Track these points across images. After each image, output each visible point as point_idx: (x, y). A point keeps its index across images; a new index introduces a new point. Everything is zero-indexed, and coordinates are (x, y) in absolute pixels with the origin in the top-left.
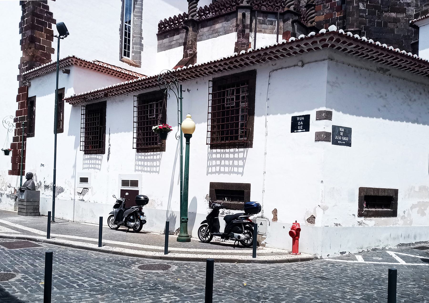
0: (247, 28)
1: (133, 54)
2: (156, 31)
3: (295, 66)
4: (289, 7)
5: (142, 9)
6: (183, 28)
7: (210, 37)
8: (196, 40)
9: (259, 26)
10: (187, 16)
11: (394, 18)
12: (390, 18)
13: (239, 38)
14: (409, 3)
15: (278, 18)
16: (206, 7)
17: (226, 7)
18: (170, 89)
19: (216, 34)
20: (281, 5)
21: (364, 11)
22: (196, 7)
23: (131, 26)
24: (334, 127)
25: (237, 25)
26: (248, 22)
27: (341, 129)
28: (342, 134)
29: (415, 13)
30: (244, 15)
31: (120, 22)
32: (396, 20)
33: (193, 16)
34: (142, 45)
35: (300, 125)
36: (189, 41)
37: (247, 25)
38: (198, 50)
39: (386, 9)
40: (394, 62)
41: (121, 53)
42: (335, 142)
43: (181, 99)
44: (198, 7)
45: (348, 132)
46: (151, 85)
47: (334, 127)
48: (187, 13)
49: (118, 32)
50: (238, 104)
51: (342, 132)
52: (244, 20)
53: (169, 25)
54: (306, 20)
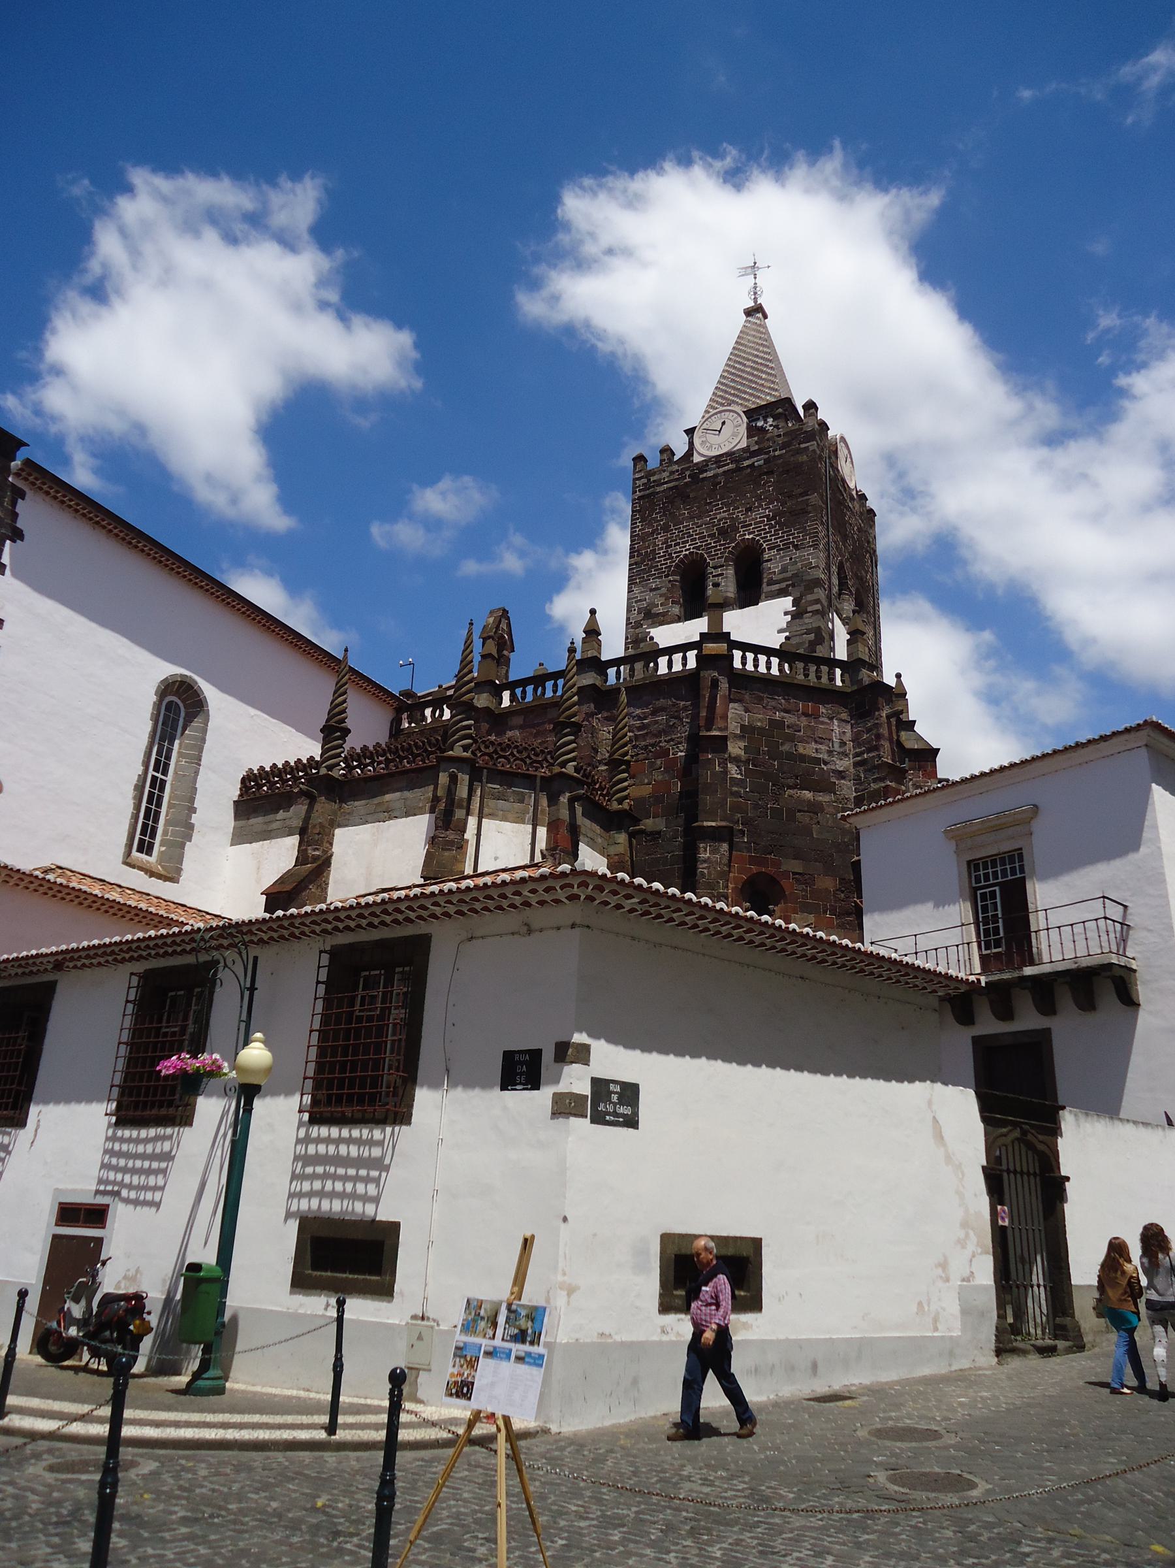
0: (461, 807)
1: (163, 849)
2: (235, 793)
3: (513, 934)
4: (563, 764)
5: (204, 740)
6: (302, 793)
7: (369, 818)
8: (334, 824)
9: (491, 803)
10: (317, 765)
12: (800, 800)
14: (841, 772)
15: (538, 788)
16: (365, 748)
17: (412, 753)
18: (226, 966)
20: (546, 759)
21: (740, 783)
22: (341, 746)
23: (169, 779)
24: (596, 1082)
25: (436, 799)
26: (462, 792)
27: (612, 1087)
28: (615, 1098)
30: (453, 779)
31: (140, 770)
32: (815, 808)
33: (330, 768)
34: (191, 827)
35: (521, 1074)
36: (314, 826)
37: (461, 799)
38: (335, 849)
39: (791, 782)
42: (598, 1119)
43: (252, 989)
44: (347, 746)
45: (630, 1093)
47: (596, 1082)
48: (318, 758)
49: (130, 792)
50: (386, 1011)
52: (453, 787)
53: (269, 781)
54: (608, 794)
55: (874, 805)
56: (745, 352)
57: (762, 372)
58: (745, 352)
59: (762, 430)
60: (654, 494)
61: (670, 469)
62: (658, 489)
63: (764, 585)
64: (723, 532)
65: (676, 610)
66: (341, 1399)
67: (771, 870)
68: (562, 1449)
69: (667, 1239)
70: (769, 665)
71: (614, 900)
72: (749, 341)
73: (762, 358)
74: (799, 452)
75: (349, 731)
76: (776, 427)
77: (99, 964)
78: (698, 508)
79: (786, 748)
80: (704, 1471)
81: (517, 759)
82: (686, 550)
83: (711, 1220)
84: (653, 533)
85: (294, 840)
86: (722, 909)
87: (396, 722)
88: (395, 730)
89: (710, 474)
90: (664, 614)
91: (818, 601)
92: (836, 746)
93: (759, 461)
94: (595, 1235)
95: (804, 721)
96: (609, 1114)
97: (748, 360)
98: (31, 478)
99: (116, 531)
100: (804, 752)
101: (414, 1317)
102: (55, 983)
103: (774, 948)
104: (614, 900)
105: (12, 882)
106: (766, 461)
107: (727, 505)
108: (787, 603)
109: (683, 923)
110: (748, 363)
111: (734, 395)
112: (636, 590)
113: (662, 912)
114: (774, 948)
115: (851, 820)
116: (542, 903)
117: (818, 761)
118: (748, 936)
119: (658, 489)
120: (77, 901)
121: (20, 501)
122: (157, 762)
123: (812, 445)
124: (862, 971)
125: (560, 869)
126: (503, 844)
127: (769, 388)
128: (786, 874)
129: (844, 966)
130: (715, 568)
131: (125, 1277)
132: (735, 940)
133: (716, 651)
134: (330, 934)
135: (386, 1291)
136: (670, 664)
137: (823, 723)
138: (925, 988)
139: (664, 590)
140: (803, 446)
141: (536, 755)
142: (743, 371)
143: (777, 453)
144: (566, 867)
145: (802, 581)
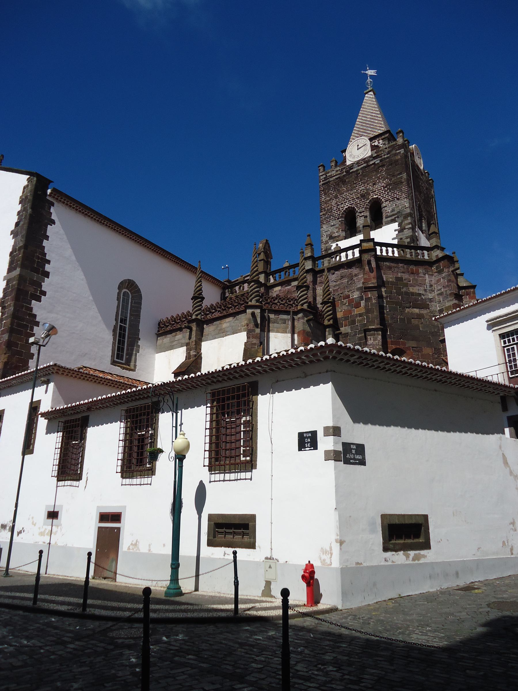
4: (302, 305)
7: (217, 336)
11: (417, 314)
13: (248, 337)
19: (223, 333)
20: (294, 303)
22: (201, 305)
24: (344, 444)
27: (352, 446)
29: (438, 309)
31: (114, 323)
32: (420, 317)
33: (197, 315)
35: (308, 443)
39: (408, 305)
40: (404, 370)
41: (113, 356)
42: (347, 462)
45: (361, 449)
46: (142, 397)
47: (344, 444)
48: (191, 312)
51: (354, 449)
55: (459, 309)
56: (366, 111)
57: (375, 120)
58: (366, 111)
59: (377, 146)
60: (329, 182)
61: (336, 169)
62: (331, 179)
63: (384, 218)
64: (363, 196)
65: (344, 234)
66: (239, 597)
67: (401, 347)
68: (346, 618)
69: (383, 516)
70: (393, 252)
71: (346, 358)
72: (368, 106)
73: (375, 113)
74: (396, 154)
75: (204, 298)
76: (384, 144)
77: (107, 407)
78: (350, 186)
79: (404, 290)
80: (420, 628)
81: (281, 304)
82: (346, 205)
83: (406, 507)
84: (330, 200)
85: (184, 349)
86: (397, 359)
87: (223, 294)
88: (223, 297)
89: (355, 170)
91: (409, 224)
92: (428, 287)
93: (377, 161)
94: (350, 517)
96: (352, 459)
97: (368, 115)
98: (56, 197)
99: (94, 217)
100: (413, 291)
101: (267, 558)
102: (88, 416)
103: (422, 376)
104: (346, 358)
105: (65, 374)
106: (381, 161)
107: (364, 183)
108: (395, 226)
109: (379, 367)
110: (368, 117)
111: (363, 132)
113: (369, 362)
114: (422, 376)
115: (439, 320)
116: (311, 362)
117: (420, 295)
118: (409, 372)
119: (331, 179)
120: (94, 380)
121: (52, 207)
123: (402, 151)
124: (464, 385)
125: (319, 344)
126: (280, 343)
127: (379, 127)
128: (408, 348)
129: (455, 383)
130: (360, 213)
131: (132, 544)
132: (403, 374)
133: (368, 247)
134: (210, 384)
135: (252, 546)
136: (347, 256)
137: (421, 277)
138: (494, 392)
139: (337, 225)
140: (397, 152)
141: (290, 302)
142: (366, 120)
143: (385, 157)
144: (322, 343)
145: (402, 215)
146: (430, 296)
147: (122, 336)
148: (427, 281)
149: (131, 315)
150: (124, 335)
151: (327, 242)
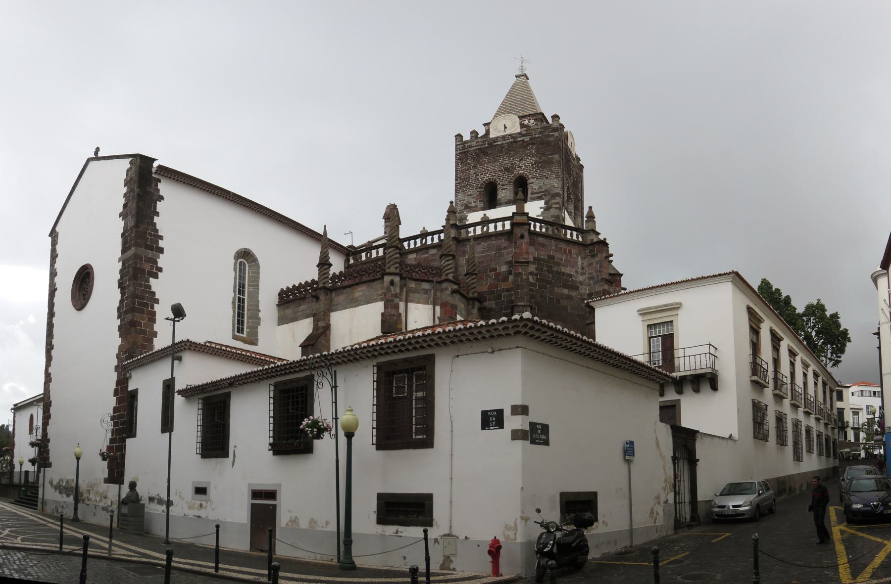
23: (246, 298)
31: (233, 294)
49: (231, 306)
65: (482, 205)
79: (555, 269)
90: (475, 207)
92: (580, 270)
95: (564, 257)
112: (460, 195)
117: (571, 276)
122: (239, 290)
146: (581, 278)
147: (241, 308)
148: (580, 263)
149: (249, 285)
150: (243, 307)
151: (461, 212)
